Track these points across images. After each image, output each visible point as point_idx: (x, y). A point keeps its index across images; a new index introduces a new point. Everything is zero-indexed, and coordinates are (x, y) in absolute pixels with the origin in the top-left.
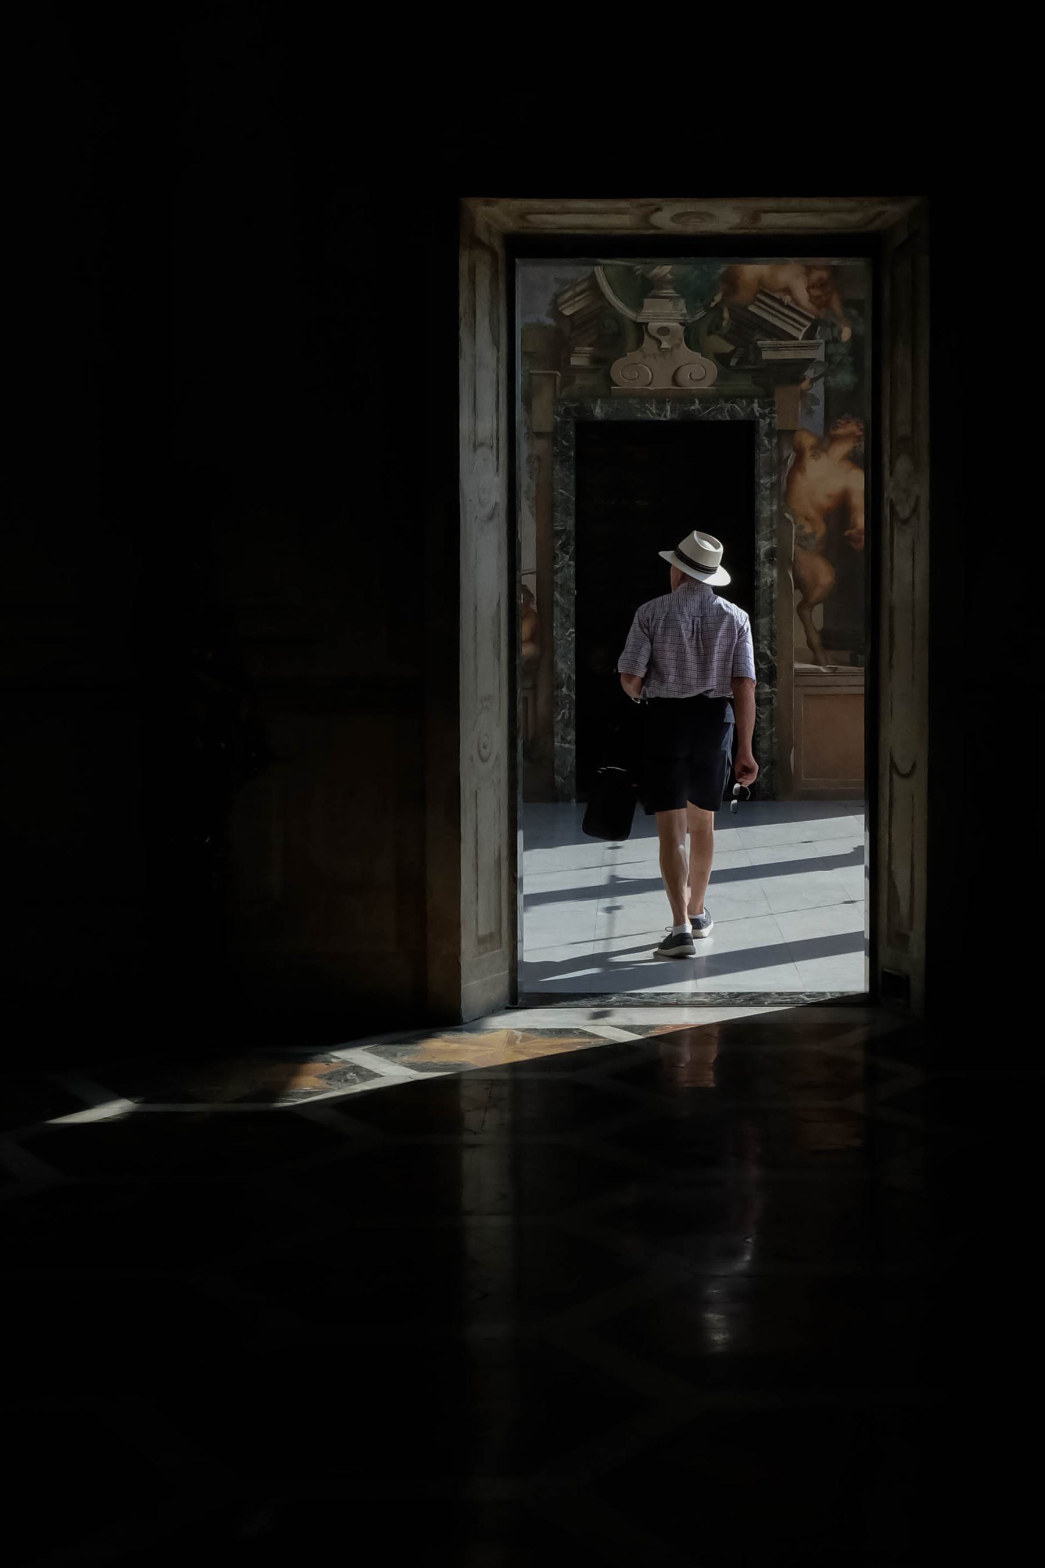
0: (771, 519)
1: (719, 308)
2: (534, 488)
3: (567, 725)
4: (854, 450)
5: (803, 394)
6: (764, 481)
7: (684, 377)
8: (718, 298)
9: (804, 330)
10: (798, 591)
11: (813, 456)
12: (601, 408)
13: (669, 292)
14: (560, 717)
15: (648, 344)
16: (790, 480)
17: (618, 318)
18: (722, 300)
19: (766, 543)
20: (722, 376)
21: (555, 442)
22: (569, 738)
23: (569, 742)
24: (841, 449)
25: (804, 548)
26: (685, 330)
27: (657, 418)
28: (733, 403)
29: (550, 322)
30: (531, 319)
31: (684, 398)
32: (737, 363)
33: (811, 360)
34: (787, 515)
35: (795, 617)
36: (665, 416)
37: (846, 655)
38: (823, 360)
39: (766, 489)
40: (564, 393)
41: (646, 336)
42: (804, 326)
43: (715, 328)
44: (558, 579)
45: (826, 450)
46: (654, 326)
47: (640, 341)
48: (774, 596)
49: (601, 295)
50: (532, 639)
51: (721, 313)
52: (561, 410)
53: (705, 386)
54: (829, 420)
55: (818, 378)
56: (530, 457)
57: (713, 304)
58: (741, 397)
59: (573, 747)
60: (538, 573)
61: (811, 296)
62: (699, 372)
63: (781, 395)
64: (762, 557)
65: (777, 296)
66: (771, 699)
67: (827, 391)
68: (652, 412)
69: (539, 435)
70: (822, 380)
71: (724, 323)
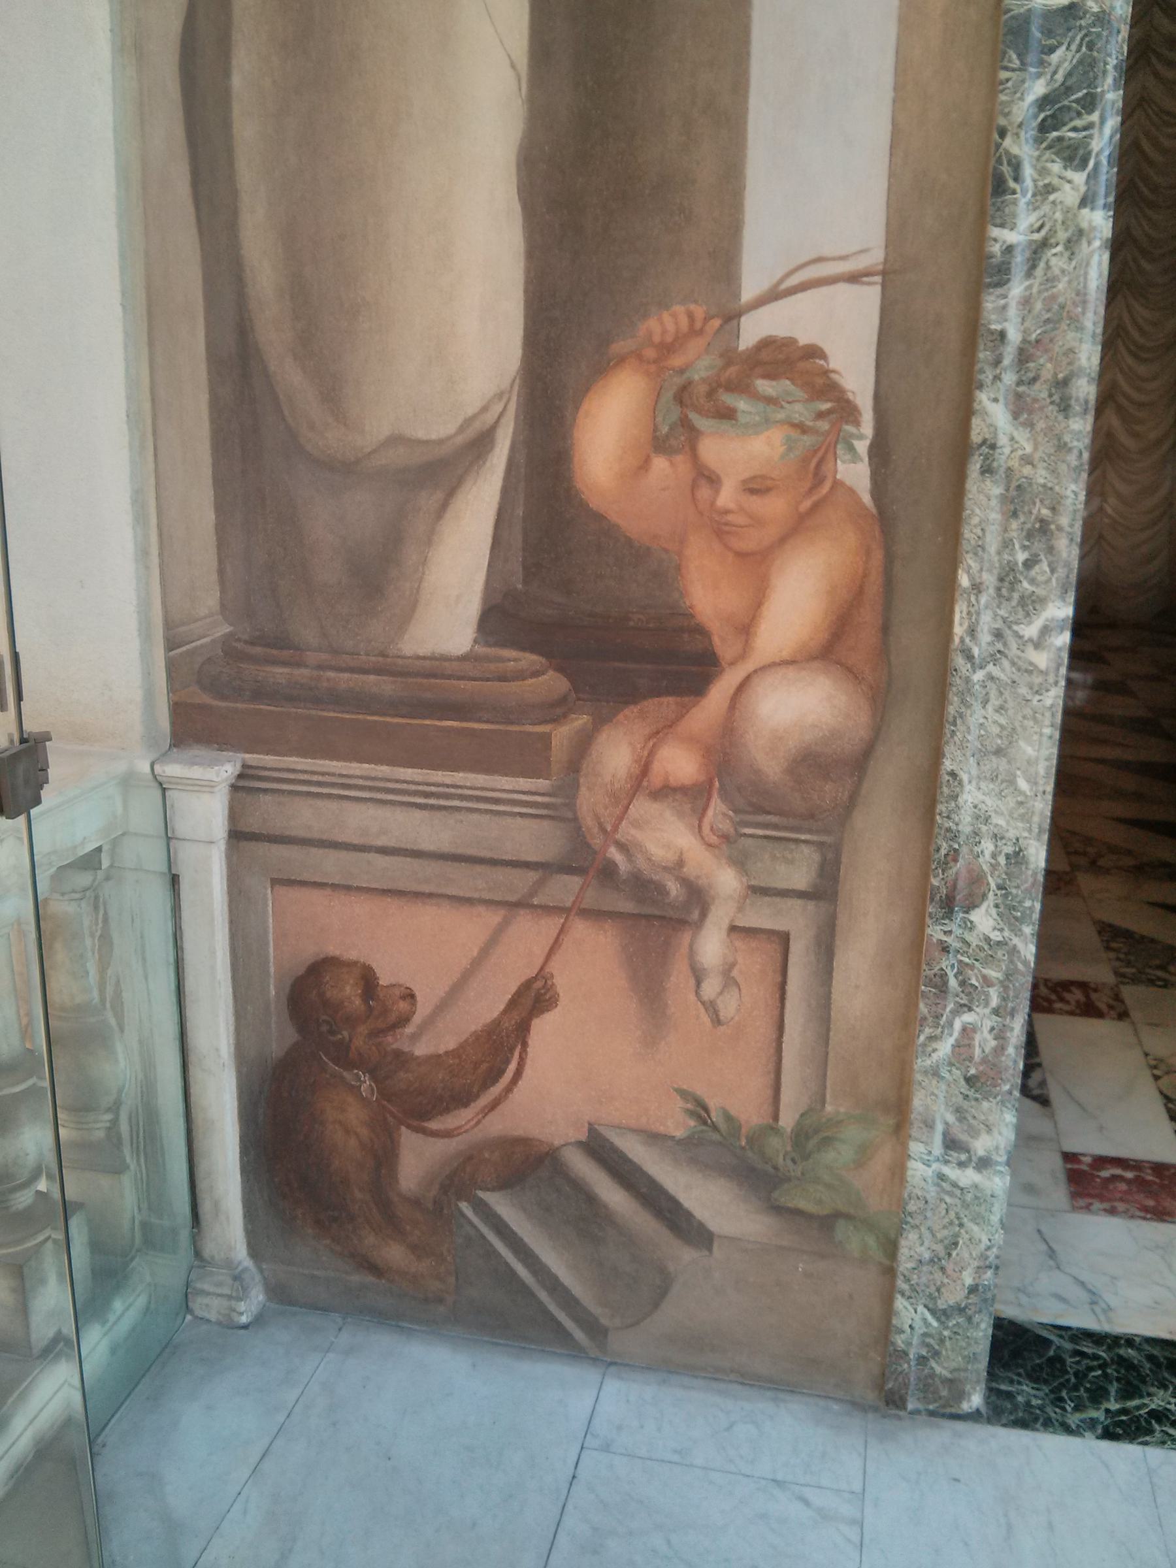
14: (945, 1048)
22: (981, 1145)
23: (984, 1164)
44: (1009, 312)
50: (828, 650)
59: (998, 1183)
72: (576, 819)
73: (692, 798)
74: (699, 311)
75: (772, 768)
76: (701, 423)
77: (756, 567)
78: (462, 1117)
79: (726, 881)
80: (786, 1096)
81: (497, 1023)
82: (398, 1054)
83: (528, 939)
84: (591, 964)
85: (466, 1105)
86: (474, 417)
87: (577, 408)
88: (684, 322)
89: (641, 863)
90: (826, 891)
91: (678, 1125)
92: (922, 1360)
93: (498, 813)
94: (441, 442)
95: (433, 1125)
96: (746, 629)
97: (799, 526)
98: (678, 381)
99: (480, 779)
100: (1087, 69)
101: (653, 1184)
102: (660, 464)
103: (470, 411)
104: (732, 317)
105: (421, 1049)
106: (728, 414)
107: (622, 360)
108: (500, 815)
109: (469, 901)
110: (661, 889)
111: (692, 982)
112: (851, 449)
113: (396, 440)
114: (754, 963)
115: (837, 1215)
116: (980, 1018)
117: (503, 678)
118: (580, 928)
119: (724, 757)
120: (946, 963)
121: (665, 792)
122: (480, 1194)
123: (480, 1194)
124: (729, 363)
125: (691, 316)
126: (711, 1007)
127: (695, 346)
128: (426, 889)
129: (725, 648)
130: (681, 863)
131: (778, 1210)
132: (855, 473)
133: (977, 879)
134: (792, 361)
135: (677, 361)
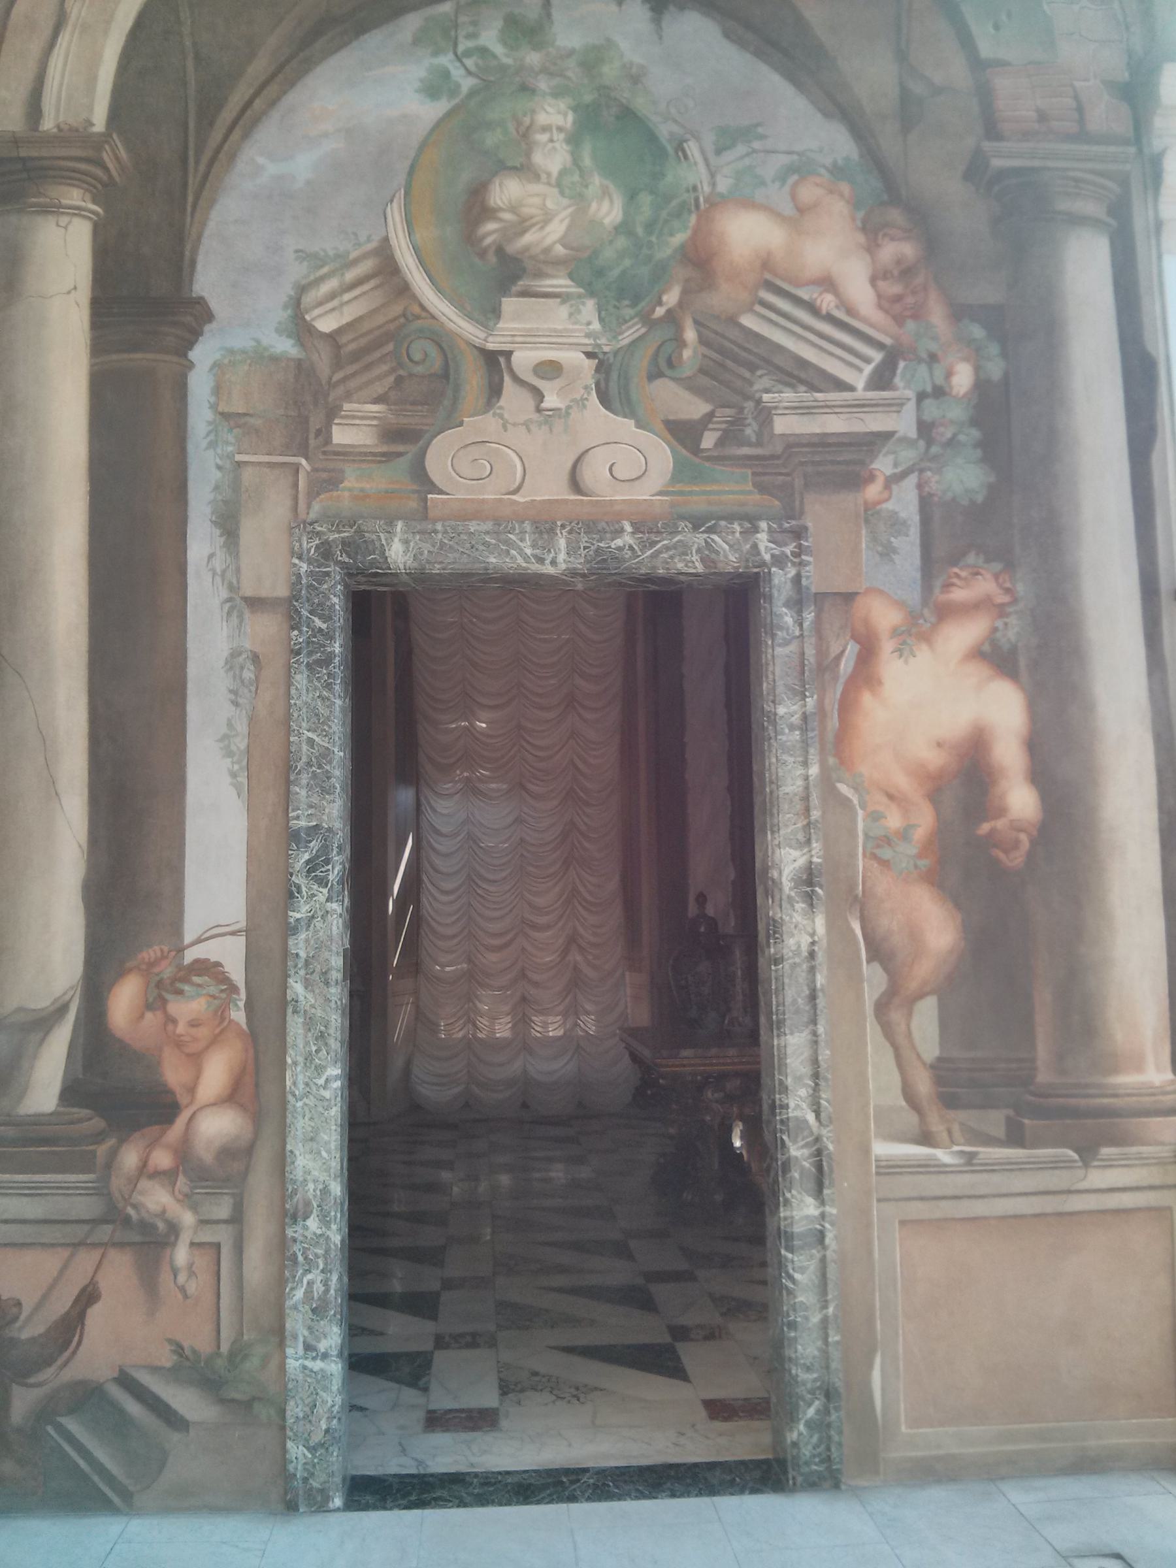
0: (806, 798)
1: (672, 318)
2: (242, 727)
4: (992, 636)
5: (870, 512)
6: (787, 710)
7: (595, 473)
8: (671, 298)
9: (868, 369)
10: (877, 967)
11: (899, 651)
12: (406, 542)
13: (560, 282)
14: (299, 1294)
15: (513, 399)
16: (847, 706)
17: (441, 339)
18: (681, 304)
19: (795, 853)
20: (681, 472)
21: (294, 622)
22: (322, 1346)
23: (325, 1356)
24: (963, 635)
25: (885, 864)
26: (597, 370)
27: (535, 567)
28: (710, 530)
30: (241, 340)
31: (595, 523)
32: (720, 443)
33: (887, 436)
34: (843, 788)
35: (872, 1028)
36: (554, 563)
37: (995, 1121)
38: (913, 433)
39: (792, 728)
40: (316, 507)
41: (507, 379)
42: (868, 361)
43: (664, 365)
44: (299, 945)
45: (926, 638)
46: (524, 359)
47: (495, 391)
48: (820, 980)
49: (404, 290)
50: (231, 1098)
51: (679, 329)
52: (309, 545)
53: (646, 492)
54: (931, 566)
55: (903, 475)
56: (235, 654)
57: (660, 312)
58: (731, 518)
60: (250, 932)
61: (879, 296)
62: (630, 464)
63: (822, 513)
64: (787, 885)
65: (804, 293)
66: (821, 1236)
67: (925, 503)
68: (521, 555)
69: (255, 603)
70: (912, 479)
71: (687, 354)
72: (109, 1194)
73: (167, 1177)
74: (166, 949)
75: (208, 1157)
76: (168, 996)
77: (196, 1060)
78: (48, 1373)
79: (188, 1218)
80: (223, 1335)
81: (68, 1313)
82: (12, 1339)
83: (86, 1261)
84: (118, 1275)
85: (50, 1365)
86: (59, 998)
87: (109, 991)
88: (159, 954)
89: (144, 1214)
90: (237, 1219)
91: (167, 1359)
92: (305, 1480)
93: (68, 1195)
94: (43, 1009)
95: (32, 1380)
96: (192, 1090)
97: (215, 1041)
98: (158, 978)
99: (60, 1177)
100: (325, 849)
101: (157, 1399)
102: (149, 1015)
103: (57, 995)
104: (181, 950)
105: (24, 1335)
106: (180, 992)
107: (130, 970)
108: (68, 1195)
109: (53, 1245)
110: (154, 1227)
111: (172, 1277)
112: (236, 1005)
113: (20, 1009)
114: (203, 1262)
115: (254, 1399)
116: (315, 1276)
117: (72, 1123)
118: (113, 1254)
119: (184, 1153)
120: (296, 1248)
121: (156, 1175)
122: (59, 1419)
123: (59, 1419)
124: (180, 970)
125: (162, 951)
126: (182, 1289)
127: (164, 963)
128: (29, 1241)
129: (183, 1099)
130: (164, 1212)
131: (222, 1401)
132: (238, 1015)
133: (308, 1204)
134: (206, 968)
135: (156, 970)
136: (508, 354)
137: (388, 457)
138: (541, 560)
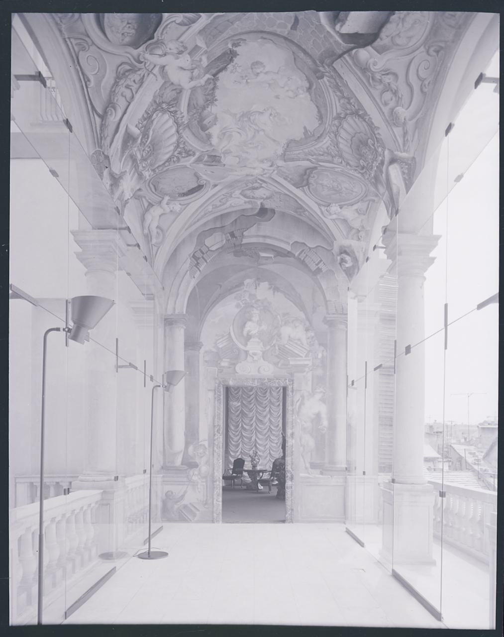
3: (218, 495)
12: (232, 381)
15: (249, 359)
29: (214, 350)
68: (250, 384)
136: (249, 351)
137: (230, 367)
138: (253, 384)
